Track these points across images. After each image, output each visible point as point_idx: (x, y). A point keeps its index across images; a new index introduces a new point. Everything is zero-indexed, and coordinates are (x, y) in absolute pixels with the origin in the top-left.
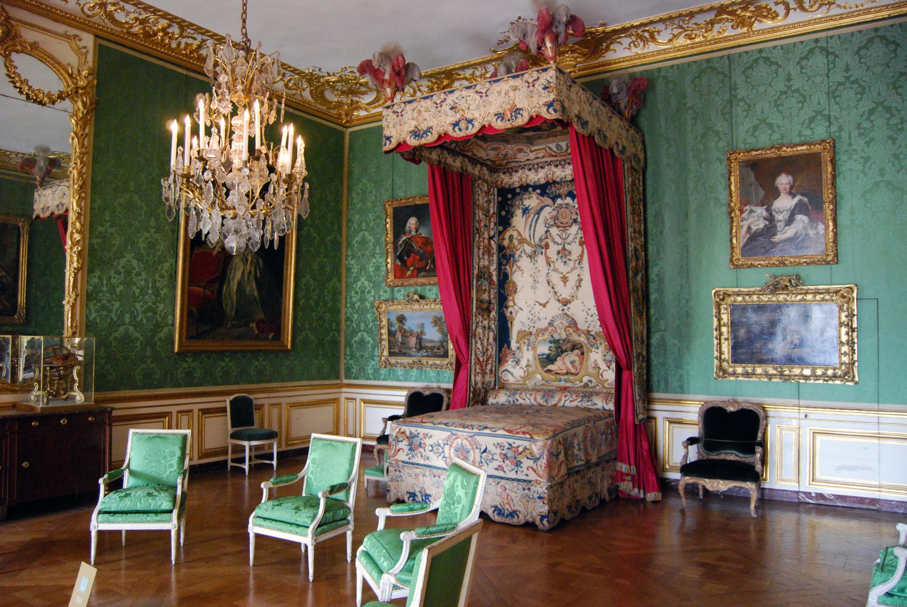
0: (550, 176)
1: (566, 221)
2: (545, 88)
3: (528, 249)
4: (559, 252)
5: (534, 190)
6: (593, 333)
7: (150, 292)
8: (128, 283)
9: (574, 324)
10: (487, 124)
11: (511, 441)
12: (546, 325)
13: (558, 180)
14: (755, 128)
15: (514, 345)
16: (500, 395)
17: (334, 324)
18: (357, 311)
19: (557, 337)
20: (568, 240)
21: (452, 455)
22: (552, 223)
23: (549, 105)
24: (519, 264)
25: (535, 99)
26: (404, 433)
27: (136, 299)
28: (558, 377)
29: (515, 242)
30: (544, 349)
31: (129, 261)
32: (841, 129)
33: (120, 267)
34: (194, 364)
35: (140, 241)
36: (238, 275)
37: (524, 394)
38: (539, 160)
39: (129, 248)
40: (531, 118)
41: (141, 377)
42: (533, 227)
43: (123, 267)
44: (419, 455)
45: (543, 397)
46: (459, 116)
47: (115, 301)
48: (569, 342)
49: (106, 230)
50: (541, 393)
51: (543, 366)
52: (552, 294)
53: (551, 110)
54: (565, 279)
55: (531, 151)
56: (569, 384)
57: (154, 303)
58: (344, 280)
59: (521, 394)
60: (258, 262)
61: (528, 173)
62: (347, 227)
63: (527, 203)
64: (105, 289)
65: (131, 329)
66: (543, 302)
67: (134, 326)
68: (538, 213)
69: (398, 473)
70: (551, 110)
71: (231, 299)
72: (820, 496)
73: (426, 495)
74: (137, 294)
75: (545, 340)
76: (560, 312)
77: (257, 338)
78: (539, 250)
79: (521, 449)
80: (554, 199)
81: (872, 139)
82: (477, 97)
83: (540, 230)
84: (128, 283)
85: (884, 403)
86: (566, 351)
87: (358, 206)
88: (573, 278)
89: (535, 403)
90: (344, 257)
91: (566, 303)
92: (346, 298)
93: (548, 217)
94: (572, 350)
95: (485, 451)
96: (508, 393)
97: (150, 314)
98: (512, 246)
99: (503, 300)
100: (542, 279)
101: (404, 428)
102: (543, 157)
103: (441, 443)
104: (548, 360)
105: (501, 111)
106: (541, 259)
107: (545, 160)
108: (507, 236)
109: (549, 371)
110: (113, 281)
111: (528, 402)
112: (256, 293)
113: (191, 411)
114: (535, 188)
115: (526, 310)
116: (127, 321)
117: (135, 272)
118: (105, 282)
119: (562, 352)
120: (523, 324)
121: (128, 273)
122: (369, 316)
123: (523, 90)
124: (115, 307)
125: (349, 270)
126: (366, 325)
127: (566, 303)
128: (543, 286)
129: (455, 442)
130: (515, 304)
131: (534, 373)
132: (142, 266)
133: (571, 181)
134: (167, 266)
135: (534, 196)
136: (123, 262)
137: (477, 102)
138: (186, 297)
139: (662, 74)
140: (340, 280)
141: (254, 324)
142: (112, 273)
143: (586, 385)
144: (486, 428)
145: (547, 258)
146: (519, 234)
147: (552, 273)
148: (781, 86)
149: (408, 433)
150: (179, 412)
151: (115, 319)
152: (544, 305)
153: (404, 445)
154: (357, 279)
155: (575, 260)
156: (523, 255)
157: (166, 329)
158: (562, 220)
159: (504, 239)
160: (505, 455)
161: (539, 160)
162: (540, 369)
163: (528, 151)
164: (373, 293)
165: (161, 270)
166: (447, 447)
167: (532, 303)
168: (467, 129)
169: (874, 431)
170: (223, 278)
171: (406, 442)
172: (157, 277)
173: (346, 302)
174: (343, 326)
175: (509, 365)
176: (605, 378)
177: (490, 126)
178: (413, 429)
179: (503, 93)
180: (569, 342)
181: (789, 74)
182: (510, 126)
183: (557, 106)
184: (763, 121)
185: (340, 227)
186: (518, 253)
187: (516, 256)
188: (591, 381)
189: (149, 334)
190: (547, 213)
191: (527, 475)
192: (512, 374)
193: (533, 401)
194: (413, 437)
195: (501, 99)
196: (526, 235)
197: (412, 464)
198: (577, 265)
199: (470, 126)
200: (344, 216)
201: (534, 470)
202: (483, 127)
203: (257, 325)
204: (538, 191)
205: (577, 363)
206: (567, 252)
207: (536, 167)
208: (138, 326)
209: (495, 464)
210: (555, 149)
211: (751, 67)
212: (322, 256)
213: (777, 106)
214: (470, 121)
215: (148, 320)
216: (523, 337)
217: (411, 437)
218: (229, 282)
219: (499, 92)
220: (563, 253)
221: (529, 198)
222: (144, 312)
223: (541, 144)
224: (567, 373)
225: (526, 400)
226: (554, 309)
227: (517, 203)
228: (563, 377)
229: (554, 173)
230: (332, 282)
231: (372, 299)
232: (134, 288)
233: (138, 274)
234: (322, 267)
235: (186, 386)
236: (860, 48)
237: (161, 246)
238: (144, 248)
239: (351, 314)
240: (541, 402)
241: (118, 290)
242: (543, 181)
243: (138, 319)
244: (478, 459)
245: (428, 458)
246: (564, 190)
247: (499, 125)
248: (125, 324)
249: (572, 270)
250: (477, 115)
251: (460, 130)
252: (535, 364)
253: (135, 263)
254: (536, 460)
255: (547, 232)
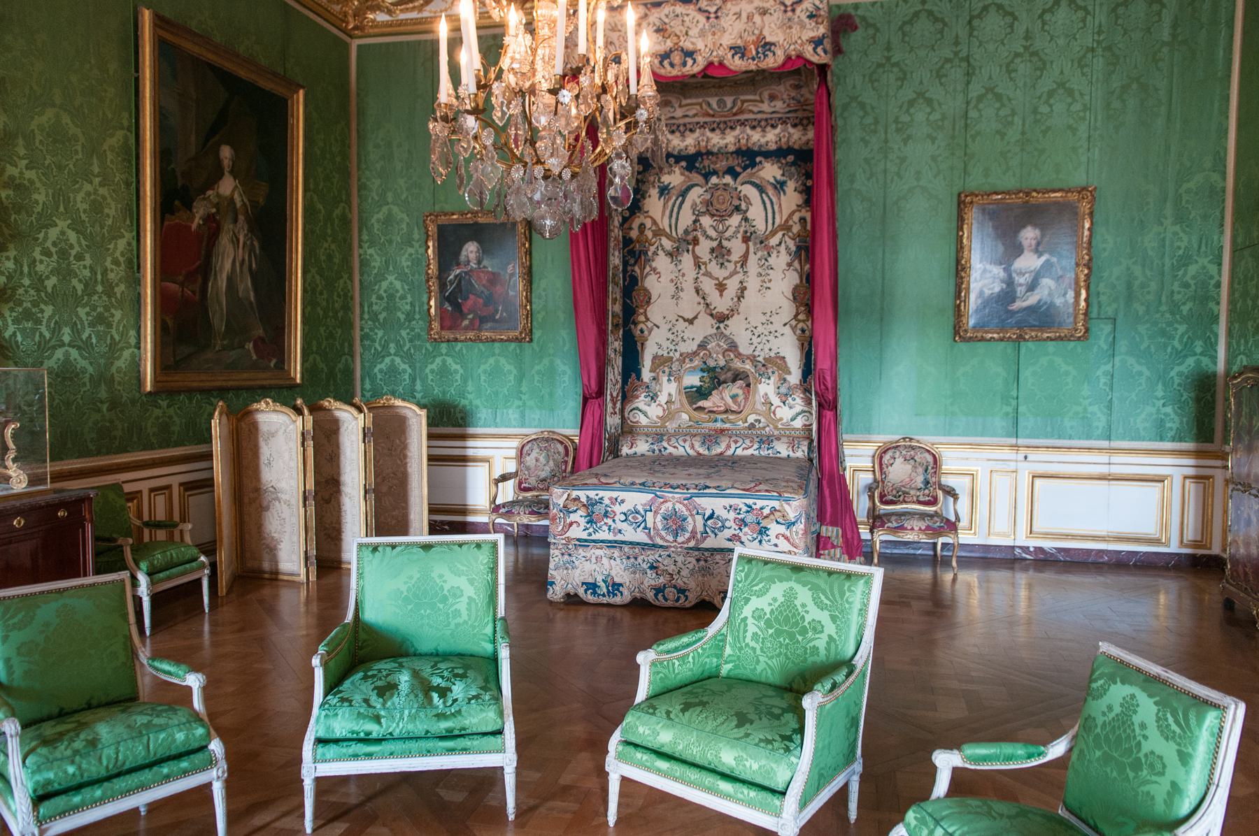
0: (743, 142)
1: (724, 207)
2: (811, 16)
3: (667, 244)
4: (712, 250)
5: (677, 162)
6: (760, 359)
7: (100, 288)
8: (65, 274)
9: (733, 347)
10: (716, 61)
11: (750, 502)
12: (695, 348)
13: (715, 150)
14: (911, 103)
15: (646, 375)
16: (638, 442)
17: (314, 342)
18: (383, 326)
19: (712, 364)
20: (727, 234)
21: (660, 526)
22: (704, 210)
23: (817, 42)
24: (654, 264)
25: (795, 31)
26: (577, 499)
27: (78, 302)
28: (713, 416)
29: (649, 234)
30: (693, 380)
31: (63, 233)
32: (1014, 113)
33: (49, 244)
34: (171, 411)
35: (79, 199)
36: (228, 266)
37: (673, 440)
38: (687, 120)
39: (62, 209)
40: (789, 58)
41: (94, 435)
42: (675, 214)
43: (54, 244)
44: (605, 528)
45: (703, 443)
46: (669, 44)
47: (46, 304)
48: (729, 370)
49: (21, 173)
50: (698, 438)
51: (691, 403)
52: (702, 307)
53: (819, 50)
54: (721, 287)
55: (680, 106)
56: (727, 426)
57: (107, 309)
58: (357, 278)
59: (669, 440)
60: (252, 244)
61: (709, 134)
62: (359, 196)
63: (666, 179)
64: (26, 282)
65: (74, 353)
66: (691, 317)
67: (79, 348)
68: (683, 194)
69: (566, 557)
70: (819, 50)
71: (220, 304)
72: (1039, 550)
73: (614, 584)
74: (80, 293)
75: (694, 368)
76: (714, 331)
77: (255, 367)
78: (684, 246)
79: (766, 511)
80: (707, 176)
81: (1049, 128)
82: (702, 19)
83: (686, 219)
84: (65, 274)
85: (1117, 439)
86: (725, 382)
87: (378, 166)
88: (733, 286)
89: (691, 452)
90: (356, 244)
91: (722, 318)
92: (362, 306)
93: (698, 202)
94: (734, 381)
95: (711, 517)
96: (650, 440)
97: (101, 328)
98: (644, 238)
99: (630, 314)
100: (688, 285)
101: (575, 494)
102: (695, 115)
103: (640, 508)
104: (697, 395)
105: (739, 42)
106: (687, 260)
107: (696, 119)
108: (635, 225)
109: (700, 409)
110: (40, 268)
111: (681, 451)
112: (252, 294)
113: (169, 487)
114: (679, 158)
115: (664, 327)
116: (67, 339)
117: (73, 252)
118: (26, 269)
119: (720, 384)
120: (660, 346)
121: (63, 254)
122: (404, 333)
123: (776, 15)
124: (46, 315)
125: (364, 263)
126: (399, 346)
127: (722, 318)
128: (689, 295)
129: (663, 507)
130: (648, 320)
131: (678, 411)
132: (84, 243)
133: (732, 153)
134: (122, 244)
135: (677, 169)
136: (53, 233)
137: (700, 26)
138: (158, 296)
139: (860, 12)
140: (351, 278)
141: (251, 345)
142: (37, 254)
143: (752, 426)
144: (707, 487)
145: (696, 257)
146: (654, 222)
147: (702, 278)
148: (947, 52)
149: (584, 499)
150: (152, 490)
151: (47, 335)
152: (691, 322)
153: (579, 516)
154: (381, 277)
155: (736, 263)
156: (660, 252)
157: (127, 354)
158: (718, 206)
159: (631, 229)
160: (743, 520)
161: (687, 120)
162: (687, 406)
163: (676, 106)
164: (409, 299)
165: (114, 251)
166: (650, 515)
167: (673, 318)
168: (684, 64)
169: (1104, 470)
170: (206, 270)
171: (582, 512)
172: (108, 264)
173: (362, 312)
174: (358, 349)
175: (641, 402)
176: (778, 416)
177: (721, 65)
178: (592, 494)
179: (744, 16)
180: (729, 370)
181: (957, 37)
182: (753, 67)
183: (827, 43)
184: (920, 94)
185: (349, 195)
186: (652, 249)
187: (650, 253)
188: (759, 421)
189: (102, 361)
190: (696, 195)
191: (776, 545)
192: (645, 414)
193: (688, 449)
194: (593, 505)
195: (740, 26)
196: (664, 224)
197: (594, 541)
198: (738, 269)
199: (690, 62)
200: (355, 179)
201: (787, 538)
202: (711, 64)
203: (255, 347)
204: (684, 164)
205: (741, 398)
206: (724, 251)
207: (682, 128)
208: (85, 347)
209: (728, 533)
210: (715, 106)
211: (910, 22)
212: (329, 239)
213: (939, 76)
214: (690, 54)
215: (100, 338)
216: (662, 364)
217: (590, 505)
218: (215, 278)
219: (738, 15)
220: (720, 252)
221: (669, 173)
222: (92, 325)
223: (697, 97)
224: (726, 411)
225: (680, 449)
226: (705, 327)
227: (652, 179)
228: (719, 417)
229: (708, 140)
230: (341, 281)
231: (408, 307)
232: (75, 282)
233: (79, 257)
234: (330, 258)
235: (161, 447)
236: (1044, 12)
237: (112, 210)
238: (85, 211)
239: (371, 329)
240: (701, 450)
241: (51, 283)
242: (692, 150)
243: (84, 336)
244: (700, 528)
245: (620, 531)
246: (721, 165)
247: (737, 64)
248: (63, 345)
249: (731, 275)
250: (700, 45)
251: (672, 65)
252: (680, 401)
253: (72, 236)
254: (790, 525)
255: (695, 221)
